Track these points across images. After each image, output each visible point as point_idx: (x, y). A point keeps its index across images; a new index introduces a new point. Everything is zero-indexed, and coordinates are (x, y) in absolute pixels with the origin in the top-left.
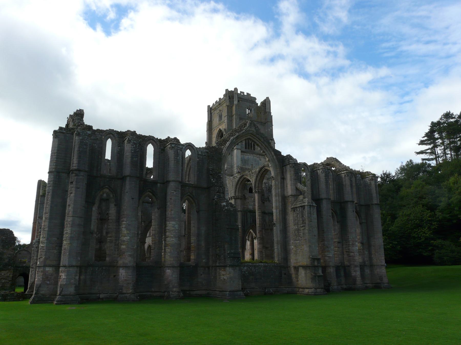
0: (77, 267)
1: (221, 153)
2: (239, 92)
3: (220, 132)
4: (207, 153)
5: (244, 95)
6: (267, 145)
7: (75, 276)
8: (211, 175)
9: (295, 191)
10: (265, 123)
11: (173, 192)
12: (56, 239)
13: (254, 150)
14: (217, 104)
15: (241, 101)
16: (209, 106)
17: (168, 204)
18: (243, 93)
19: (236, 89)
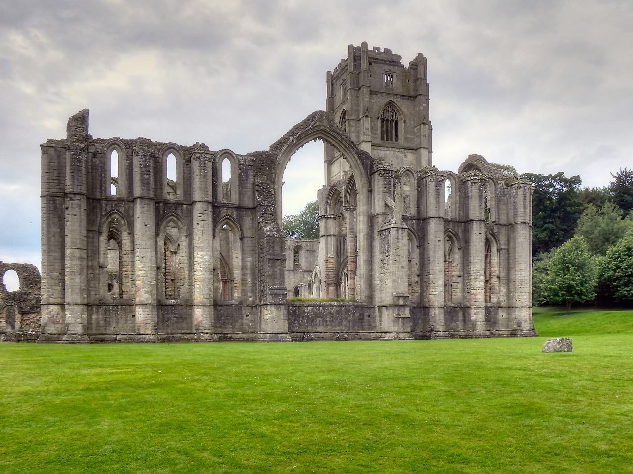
0: (83, 304)
1: (273, 162)
2: (370, 48)
3: (344, 113)
4: (253, 161)
5: (380, 53)
6: (347, 145)
7: (82, 314)
8: (257, 191)
9: (384, 208)
10: (416, 97)
11: (200, 215)
12: (58, 274)
13: (397, 140)
14: (340, 70)
15: (375, 62)
16: (329, 73)
17: (195, 230)
18: (379, 49)
19: (365, 44)
